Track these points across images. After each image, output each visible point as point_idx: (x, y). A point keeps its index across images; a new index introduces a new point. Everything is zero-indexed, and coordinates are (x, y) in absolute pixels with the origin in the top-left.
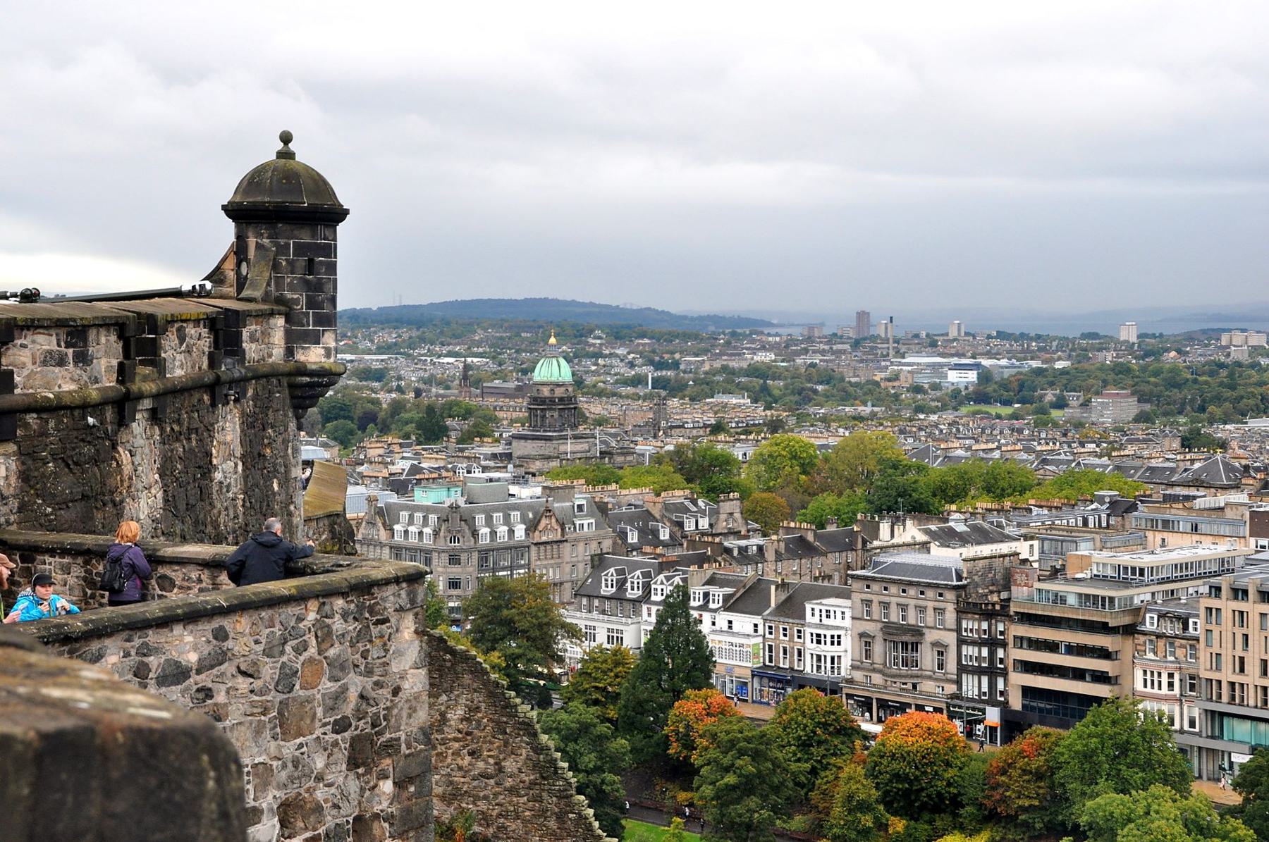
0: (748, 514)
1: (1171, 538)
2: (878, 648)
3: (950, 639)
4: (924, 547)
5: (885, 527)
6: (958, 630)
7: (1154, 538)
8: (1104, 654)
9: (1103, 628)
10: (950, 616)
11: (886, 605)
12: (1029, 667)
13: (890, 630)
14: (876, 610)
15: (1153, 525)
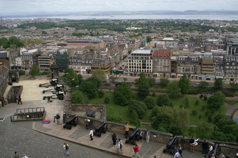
0: (4, 48)
1: (49, 47)
2: (24, 63)
3: (32, 61)
4: (27, 51)
5: (21, 49)
6: (33, 60)
7: (48, 47)
8: (48, 61)
9: (48, 58)
10: (32, 59)
11: (25, 58)
12: (41, 63)
13: (25, 61)
14: (24, 59)
15: (48, 45)
